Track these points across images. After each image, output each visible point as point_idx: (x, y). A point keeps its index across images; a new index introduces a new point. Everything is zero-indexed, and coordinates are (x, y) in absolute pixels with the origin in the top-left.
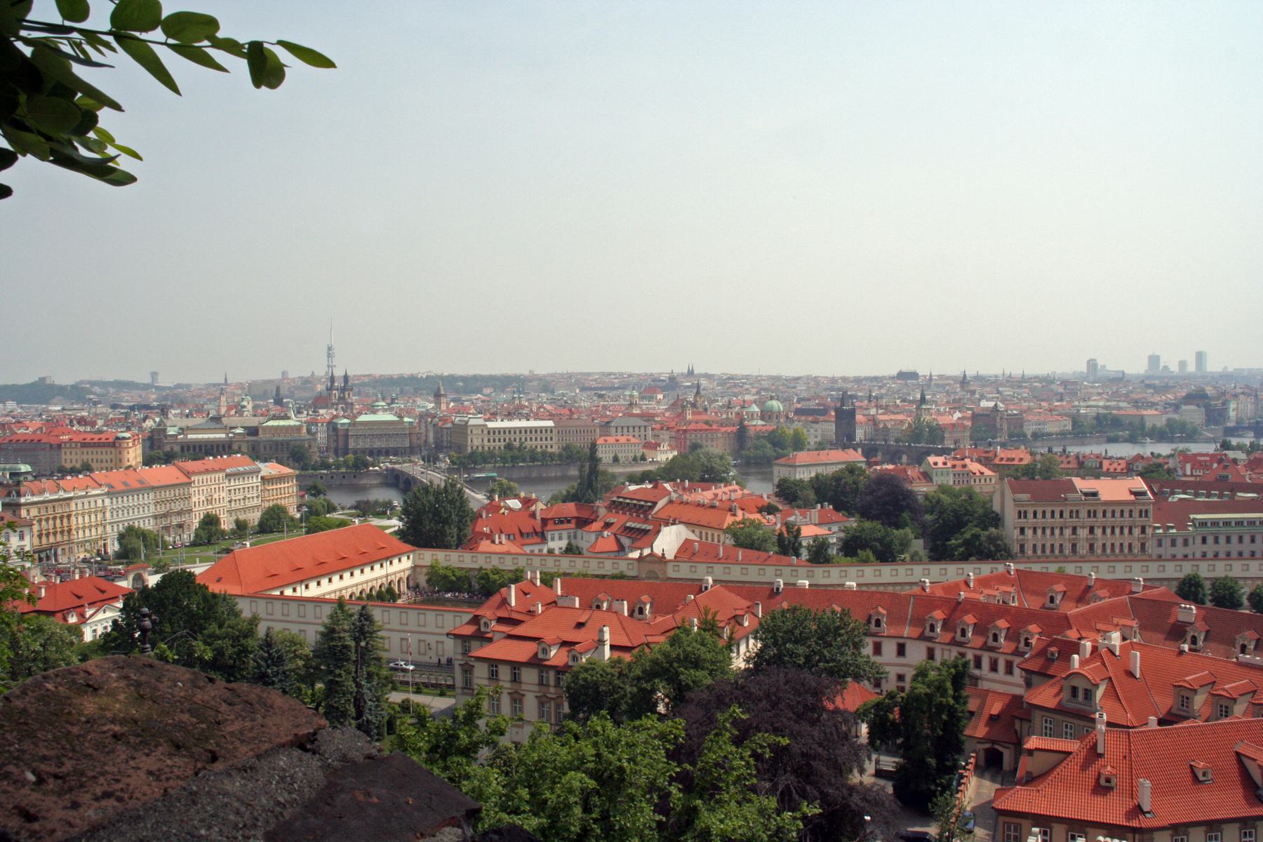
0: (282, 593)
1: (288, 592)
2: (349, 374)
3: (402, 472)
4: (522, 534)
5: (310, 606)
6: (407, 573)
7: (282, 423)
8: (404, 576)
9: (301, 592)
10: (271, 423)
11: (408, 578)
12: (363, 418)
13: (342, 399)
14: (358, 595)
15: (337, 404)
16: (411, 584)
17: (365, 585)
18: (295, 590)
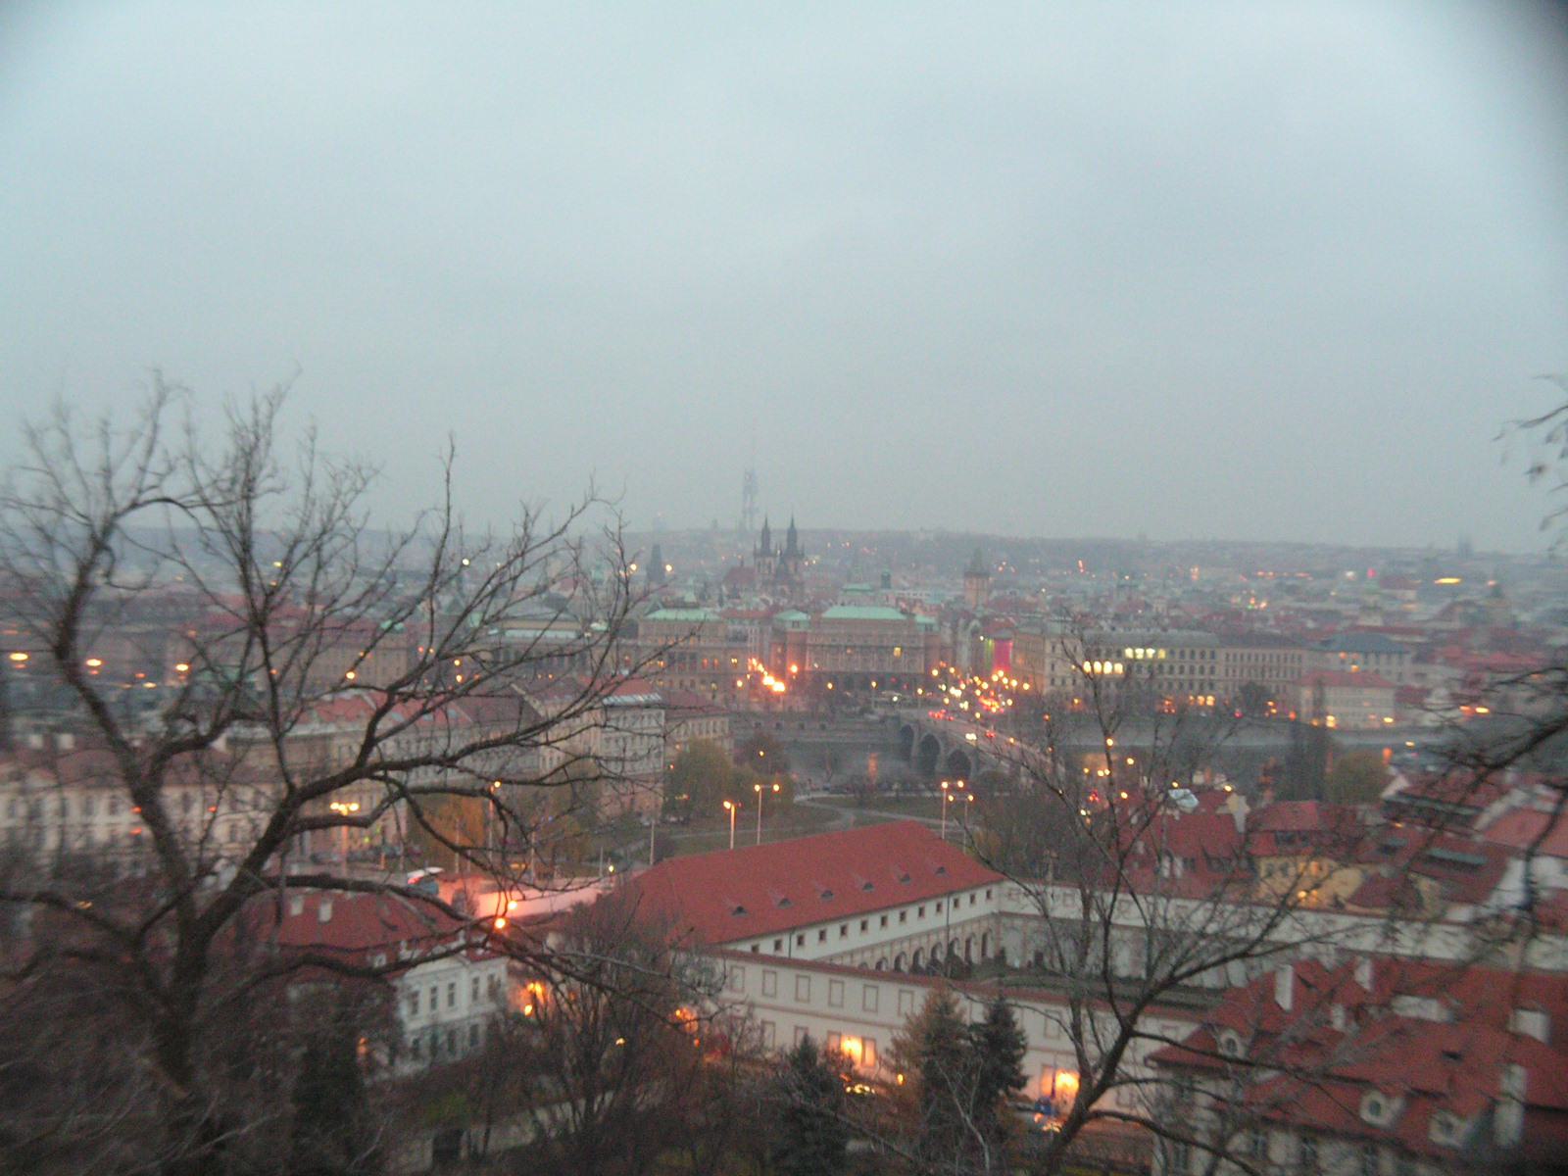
0: (755, 949)
1: (766, 947)
2: (798, 526)
3: (917, 722)
4: (1209, 859)
5: (820, 981)
6: (985, 924)
7: (683, 615)
8: (978, 930)
9: (789, 948)
10: (661, 614)
11: (984, 937)
12: (834, 612)
13: (782, 575)
14: (892, 965)
15: (774, 584)
16: (990, 954)
17: (887, 950)
18: (778, 945)
